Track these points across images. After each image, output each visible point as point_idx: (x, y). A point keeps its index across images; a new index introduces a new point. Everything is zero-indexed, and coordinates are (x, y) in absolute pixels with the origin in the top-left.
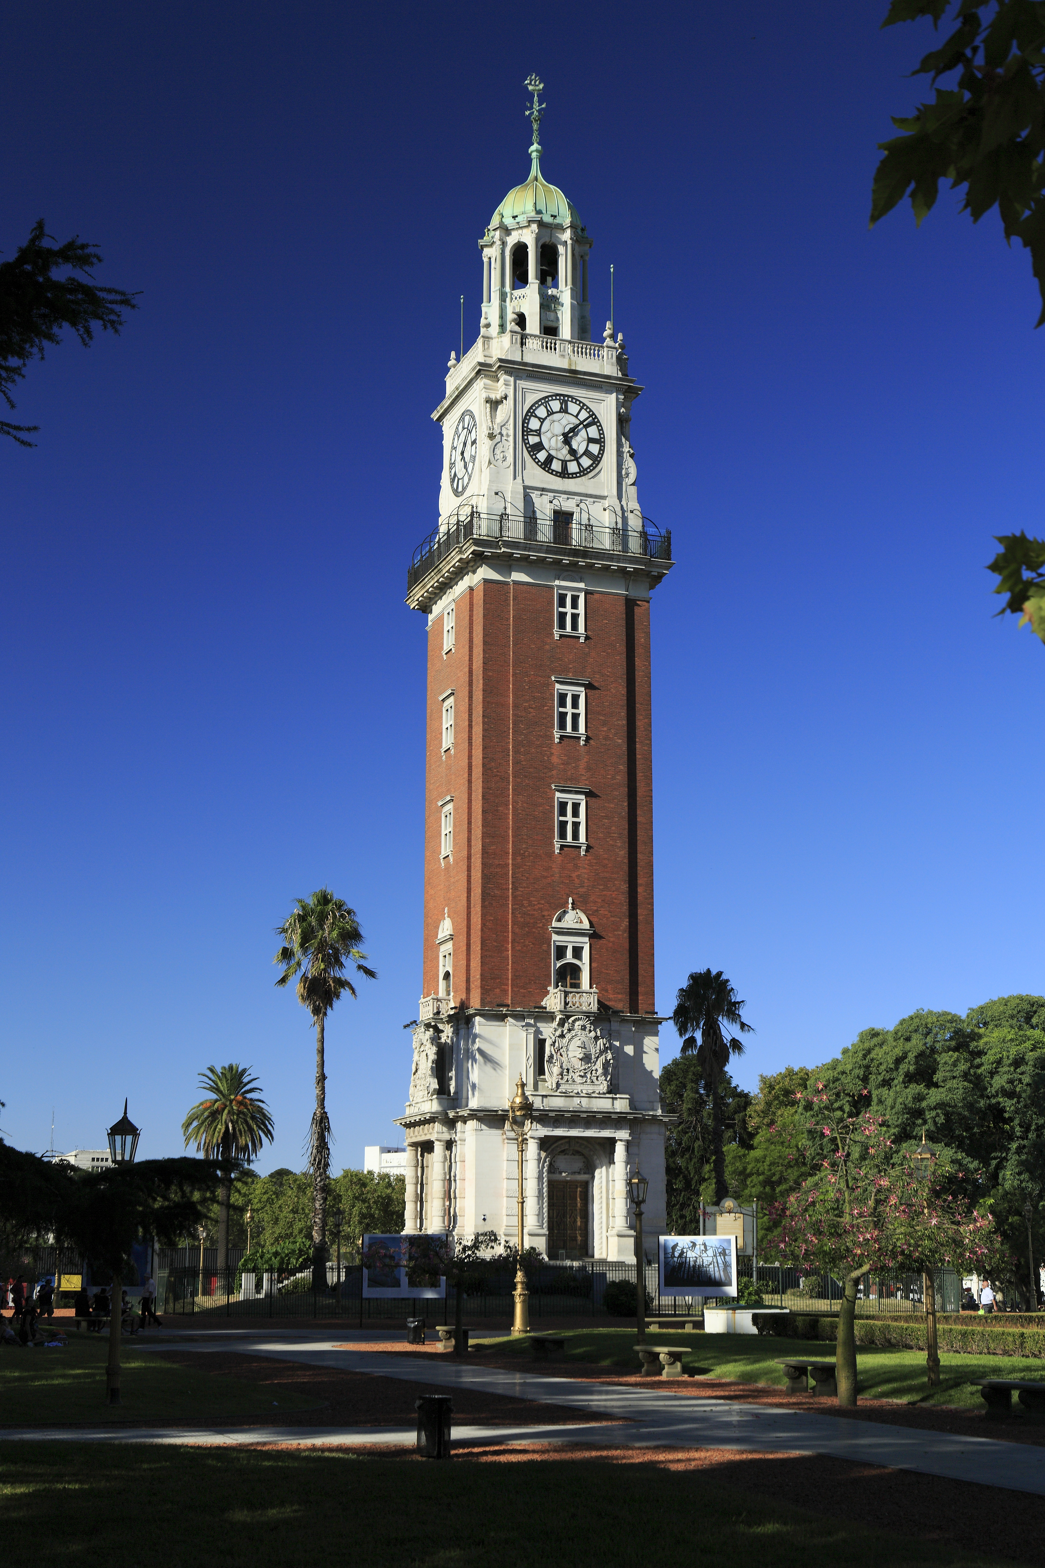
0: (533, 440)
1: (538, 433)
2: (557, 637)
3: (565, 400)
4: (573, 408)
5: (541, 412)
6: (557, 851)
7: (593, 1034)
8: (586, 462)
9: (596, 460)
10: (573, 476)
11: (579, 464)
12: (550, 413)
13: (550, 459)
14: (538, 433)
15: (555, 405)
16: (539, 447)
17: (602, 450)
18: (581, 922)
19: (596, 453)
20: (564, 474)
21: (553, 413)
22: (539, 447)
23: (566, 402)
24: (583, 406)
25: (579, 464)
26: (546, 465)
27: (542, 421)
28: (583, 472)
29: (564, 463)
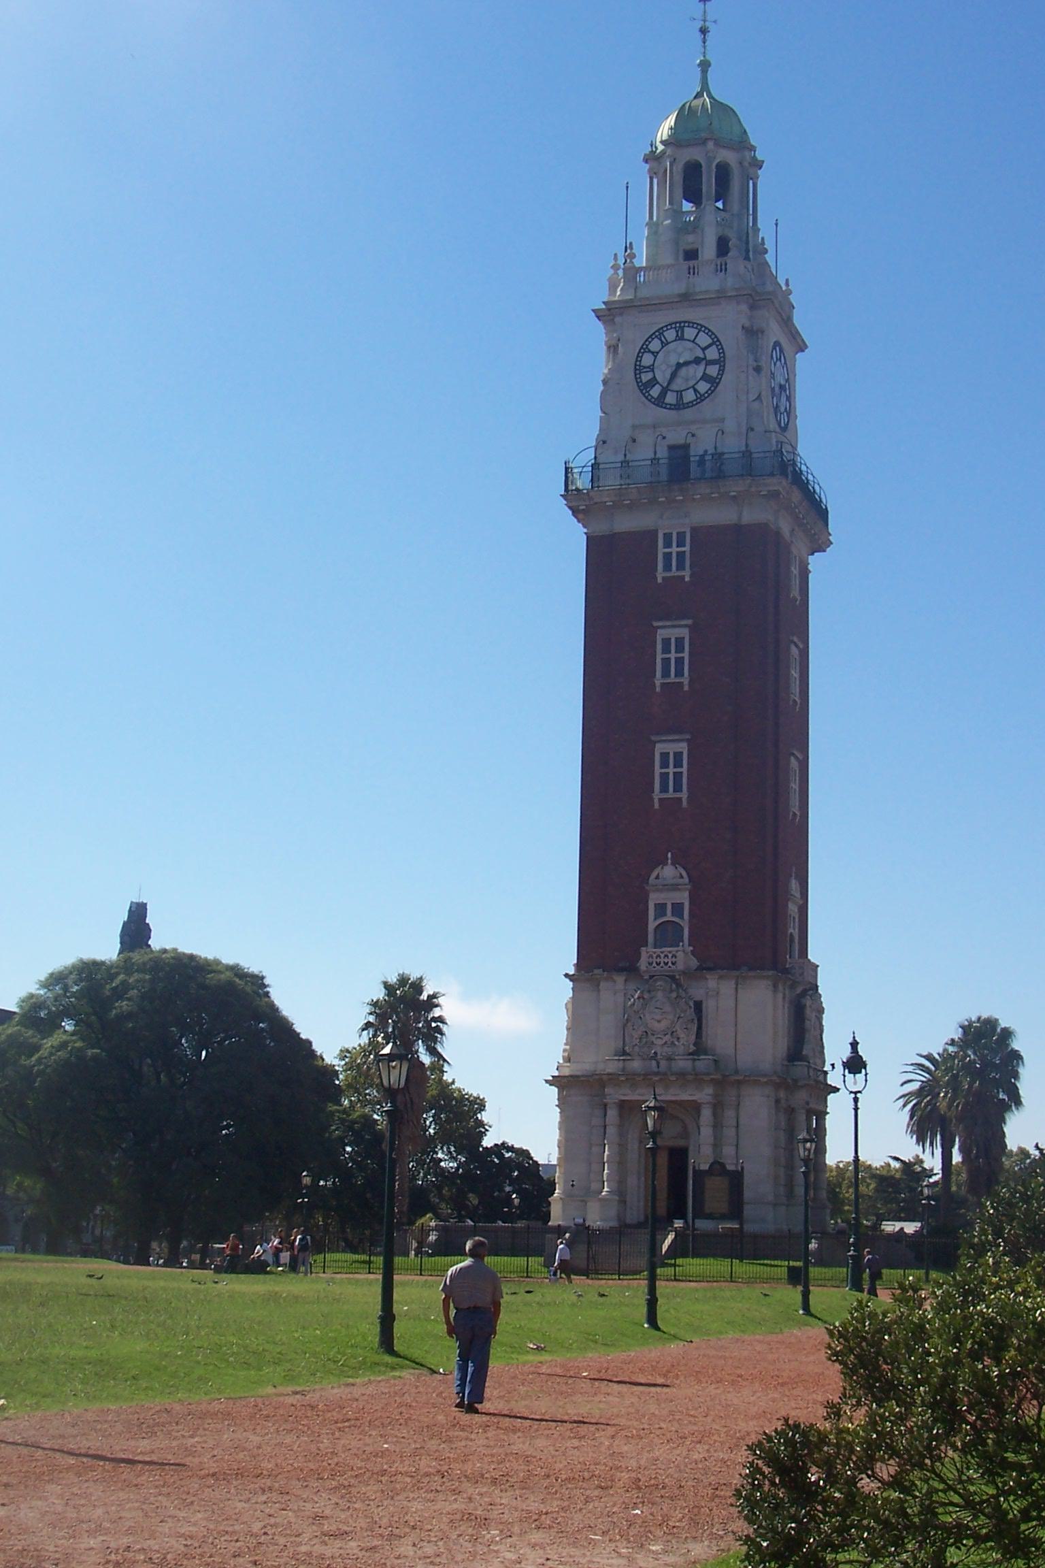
0: (646, 377)
1: (651, 368)
2: (660, 580)
3: (679, 327)
4: (689, 333)
5: (655, 345)
6: (657, 806)
7: (674, 995)
8: (703, 387)
9: (714, 382)
10: (691, 405)
11: (695, 390)
12: (665, 344)
13: (664, 392)
14: (651, 368)
15: (670, 335)
16: (653, 382)
17: (722, 371)
18: (682, 877)
19: (715, 375)
20: (679, 406)
21: (668, 343)
22: (653, 382)
23: (682, 328)
24: (701, 328)
25: (695, 390)
26: (659, 402)
27: (655, 354)
28: (701, 398)
29: (680, 393)
